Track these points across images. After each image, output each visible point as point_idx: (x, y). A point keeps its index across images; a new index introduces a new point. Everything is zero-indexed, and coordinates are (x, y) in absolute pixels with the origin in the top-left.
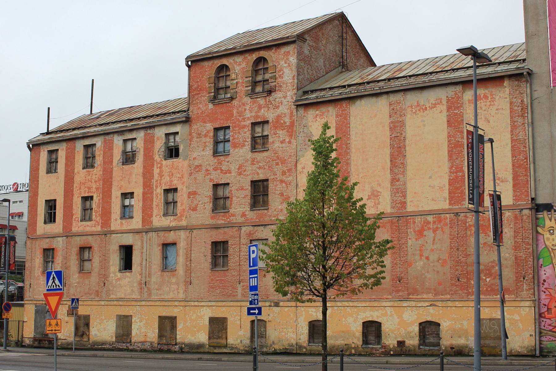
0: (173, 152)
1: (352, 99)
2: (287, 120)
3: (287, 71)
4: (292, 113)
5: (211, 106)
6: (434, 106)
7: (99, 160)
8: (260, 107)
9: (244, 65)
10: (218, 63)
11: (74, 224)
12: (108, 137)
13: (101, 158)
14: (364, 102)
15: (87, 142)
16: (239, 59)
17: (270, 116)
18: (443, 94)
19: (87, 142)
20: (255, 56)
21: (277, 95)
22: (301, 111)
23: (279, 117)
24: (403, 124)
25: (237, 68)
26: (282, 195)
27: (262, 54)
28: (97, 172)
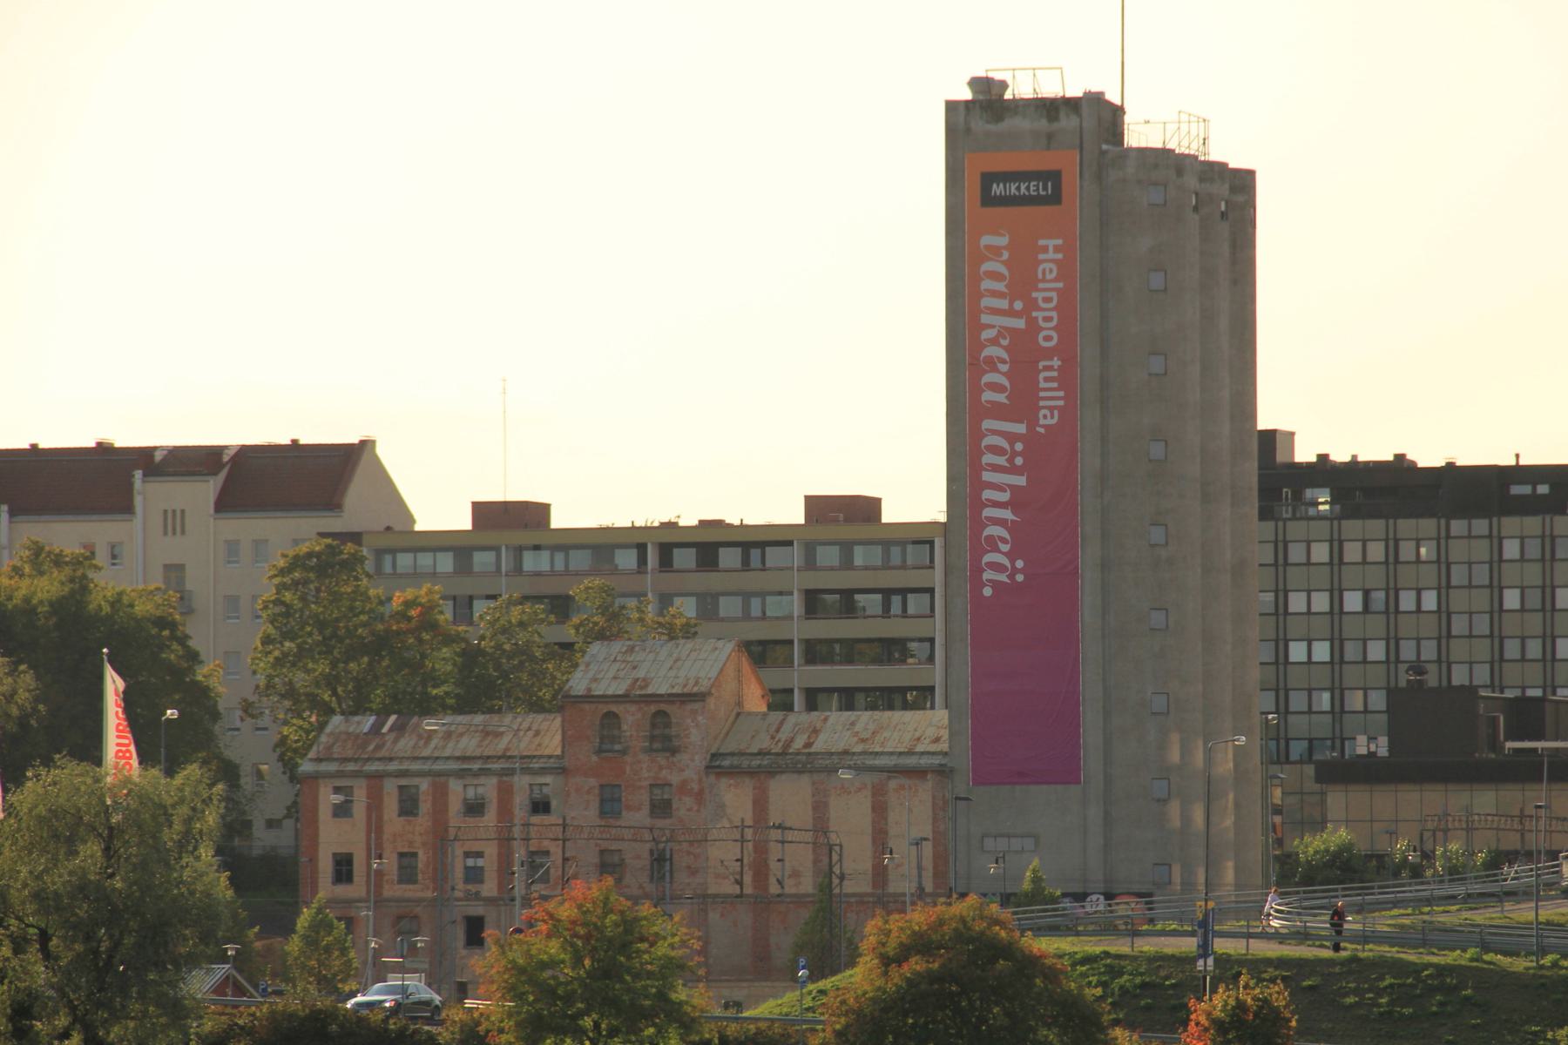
0: (540, 806)
1: (771, 773)
2: (696, 787)
3: (694, 731)
4: (700, 781)
5: (594, 758)
6: (860, 790)
7: (425, 806)
8: (661, 768)
9: (639, 716)
10: (604, 709)
11: (386, 887)
12: (442, 779)
13: (429, 805)
14: (784, 777)
15: (404, 782)
16: (633, 708)
17: (675, 779)
18: (869, 779)
19: (404, 782)
20: (653, 708)
21: (683, 758)
22: (712, 778)
23: (684, 783)
24: (826, 805)
25: (630, 719)
26: (689, 867)
27: (663, 707)
28: (423, 821)
